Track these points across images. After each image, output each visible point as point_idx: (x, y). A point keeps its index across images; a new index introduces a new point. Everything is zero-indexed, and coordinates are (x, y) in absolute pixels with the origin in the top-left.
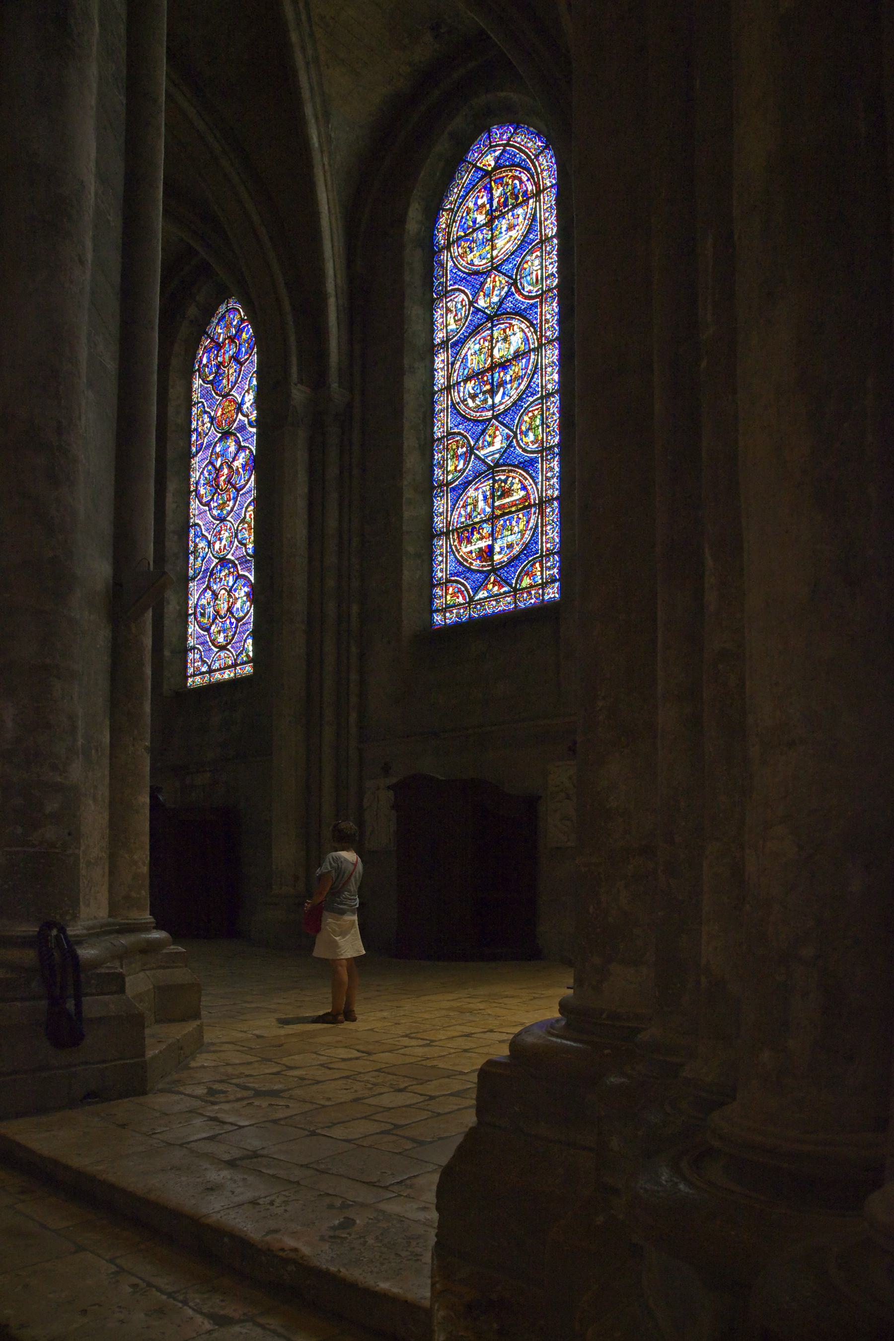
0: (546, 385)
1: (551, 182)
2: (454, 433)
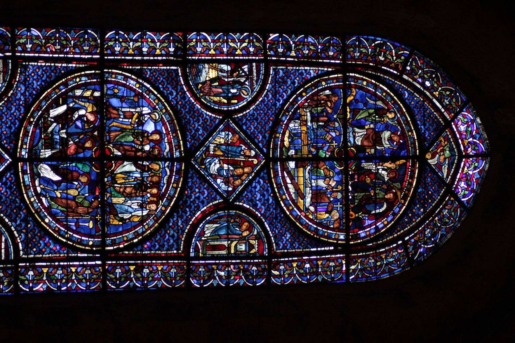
0: (34, 268)
1: (354, 270)
2: (13, 76)
